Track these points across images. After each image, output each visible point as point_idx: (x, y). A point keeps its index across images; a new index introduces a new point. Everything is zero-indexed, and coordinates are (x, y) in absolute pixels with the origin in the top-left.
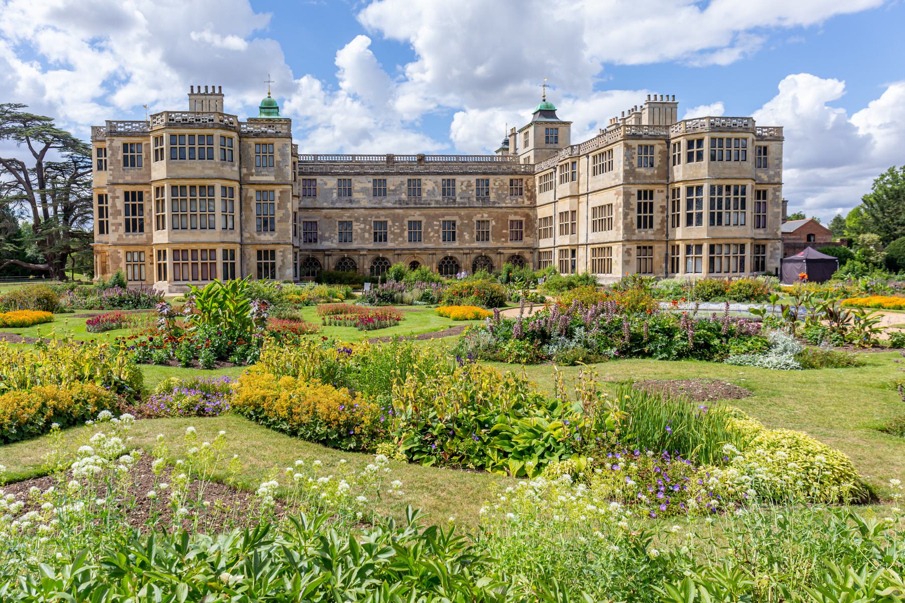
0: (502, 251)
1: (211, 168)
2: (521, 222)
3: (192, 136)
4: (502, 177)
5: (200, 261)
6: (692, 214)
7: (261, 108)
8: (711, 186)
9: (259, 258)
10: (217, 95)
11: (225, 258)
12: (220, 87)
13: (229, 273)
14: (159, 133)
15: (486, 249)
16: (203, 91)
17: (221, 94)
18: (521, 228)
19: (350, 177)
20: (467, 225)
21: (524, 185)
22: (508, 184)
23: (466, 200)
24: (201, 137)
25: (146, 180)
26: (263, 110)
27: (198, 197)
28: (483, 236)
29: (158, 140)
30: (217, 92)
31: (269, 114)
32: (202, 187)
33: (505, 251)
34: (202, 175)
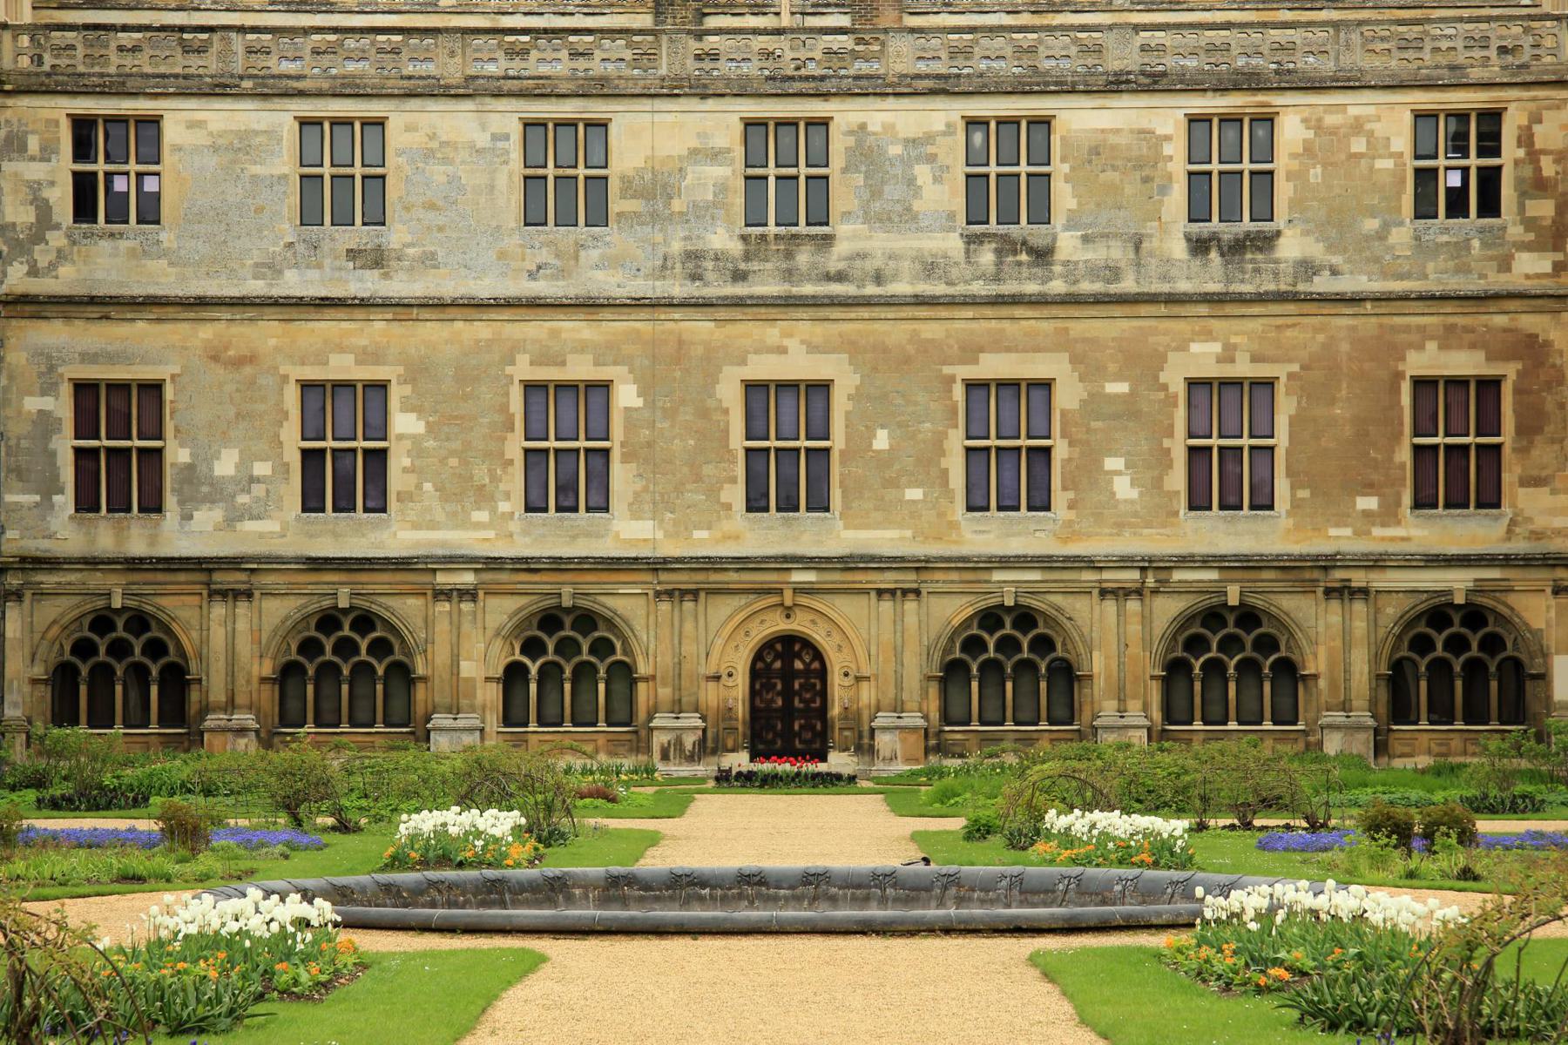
4: (1358, 105)
15: (1248, 564)
19: (373, 109)
22: (1402, 142)
23: (1117, 252)
28: (1222, 479)
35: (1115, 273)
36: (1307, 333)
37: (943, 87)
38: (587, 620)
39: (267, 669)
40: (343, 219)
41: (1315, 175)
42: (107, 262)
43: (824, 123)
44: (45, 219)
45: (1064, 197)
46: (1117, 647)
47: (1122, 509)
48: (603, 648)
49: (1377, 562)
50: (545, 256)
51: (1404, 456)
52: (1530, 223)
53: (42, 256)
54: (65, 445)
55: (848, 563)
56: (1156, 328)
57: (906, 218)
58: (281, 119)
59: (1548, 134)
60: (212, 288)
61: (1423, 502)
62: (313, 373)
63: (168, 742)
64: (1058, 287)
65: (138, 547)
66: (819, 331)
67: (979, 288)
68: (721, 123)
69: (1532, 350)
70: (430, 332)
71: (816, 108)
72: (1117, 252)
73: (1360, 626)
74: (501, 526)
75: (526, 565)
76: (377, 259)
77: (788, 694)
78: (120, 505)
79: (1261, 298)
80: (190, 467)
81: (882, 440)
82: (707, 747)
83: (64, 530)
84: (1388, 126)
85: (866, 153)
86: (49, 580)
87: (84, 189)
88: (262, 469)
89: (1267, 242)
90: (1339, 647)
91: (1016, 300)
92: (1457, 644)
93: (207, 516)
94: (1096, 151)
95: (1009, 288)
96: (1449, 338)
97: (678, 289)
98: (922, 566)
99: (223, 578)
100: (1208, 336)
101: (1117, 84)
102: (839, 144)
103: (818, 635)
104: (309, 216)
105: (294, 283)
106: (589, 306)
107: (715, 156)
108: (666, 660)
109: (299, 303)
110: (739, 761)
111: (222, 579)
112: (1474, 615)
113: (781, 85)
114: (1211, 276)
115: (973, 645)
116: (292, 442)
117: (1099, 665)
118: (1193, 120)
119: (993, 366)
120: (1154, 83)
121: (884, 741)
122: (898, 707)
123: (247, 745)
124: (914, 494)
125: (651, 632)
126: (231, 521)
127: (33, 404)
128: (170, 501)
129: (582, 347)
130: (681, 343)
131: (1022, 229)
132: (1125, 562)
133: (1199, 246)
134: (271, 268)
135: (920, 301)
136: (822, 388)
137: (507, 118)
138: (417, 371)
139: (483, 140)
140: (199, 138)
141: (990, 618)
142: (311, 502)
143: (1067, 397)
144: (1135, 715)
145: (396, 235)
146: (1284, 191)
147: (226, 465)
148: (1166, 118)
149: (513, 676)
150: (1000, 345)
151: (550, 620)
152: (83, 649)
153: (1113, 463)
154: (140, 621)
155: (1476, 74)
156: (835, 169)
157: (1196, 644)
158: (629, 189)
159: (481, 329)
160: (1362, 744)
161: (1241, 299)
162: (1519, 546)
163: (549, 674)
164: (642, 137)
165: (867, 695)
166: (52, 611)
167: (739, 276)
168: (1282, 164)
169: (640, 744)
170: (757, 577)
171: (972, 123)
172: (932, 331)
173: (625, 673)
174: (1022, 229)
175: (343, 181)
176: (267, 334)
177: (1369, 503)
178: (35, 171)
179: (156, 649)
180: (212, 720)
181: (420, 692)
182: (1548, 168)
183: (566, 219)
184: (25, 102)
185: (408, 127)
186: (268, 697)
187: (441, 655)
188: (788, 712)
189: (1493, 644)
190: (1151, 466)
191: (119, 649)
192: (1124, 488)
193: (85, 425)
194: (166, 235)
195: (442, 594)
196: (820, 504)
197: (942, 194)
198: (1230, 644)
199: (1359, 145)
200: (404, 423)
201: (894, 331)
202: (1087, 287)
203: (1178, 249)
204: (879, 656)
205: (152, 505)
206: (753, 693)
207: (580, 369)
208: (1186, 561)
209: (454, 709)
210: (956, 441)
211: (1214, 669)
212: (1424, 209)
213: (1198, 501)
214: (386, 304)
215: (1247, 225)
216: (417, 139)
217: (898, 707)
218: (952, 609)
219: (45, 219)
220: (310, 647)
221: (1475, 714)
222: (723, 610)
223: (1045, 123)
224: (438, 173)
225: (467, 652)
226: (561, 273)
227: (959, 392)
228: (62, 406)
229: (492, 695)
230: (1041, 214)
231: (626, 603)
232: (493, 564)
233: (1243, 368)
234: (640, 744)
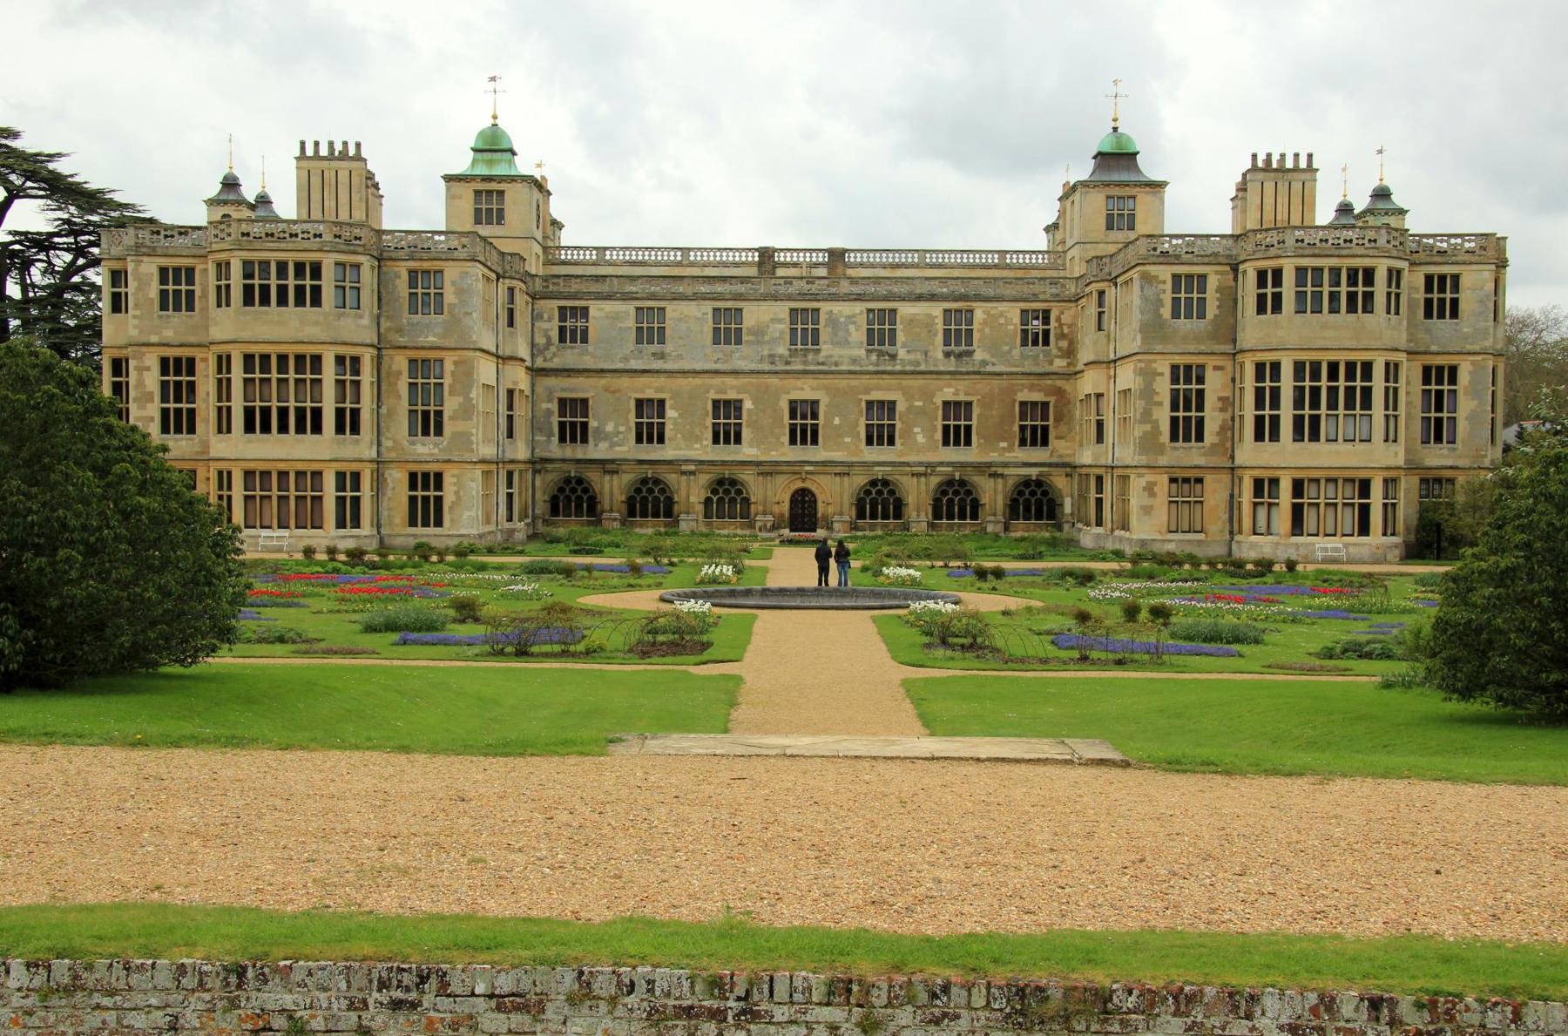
0: (1000, 470)
1: (317, 323)
2: (1045, 405)
3: (282, 267)
4: (1002, 307)
5: (293, 493)
6: (1303, 416)
7: (475, 150)
8: (1296, 363)
9: (413, 486)
10: (352, 159)
11: (341, 486)
12: (358, 145)
13: (349, 514)
14: (223, 256)
16: (324, 152)
17: (358, 157)
18: (1045, 417)
20: (922, 412)
21: (1053, 324)
22: (1017, 320)
24: (300, 268)
25: (204, 340)
26: (479, 155)
27: (292, 375)
28: (957, 435)
29: (223, 268)
30: (352, 152)
31: (490, 163)
32: (300, 358)
33: (1007, 471)
34: (300, 336)
35: (918, 364)
36: (984, 386)
37: (859, 298)
38: (733, 482)
39: (623, 498)
40: (651, 342)
41: (987, 330)
42: (571, 356)
43: (818, 310)
44: (549, 343)
45: (901, 337)
46: (917, 495)
47: (920, 447)
48: (739, 492)
49: (1006, 465)
50: (720, 355)
51: (1016, 428)
52: (1060, 349)
53: (548, 355)
54: (555, 420)
55: (824, 463)
56: (932, 383)
57: (845, 343)
58: (629, 308)
59: (1066, 318)
60: (606, 366)
61: (1023, 443)
62: (640, 396)
63: (590, 523)
64: (898, 368)
65: (580, 456)
66: (816, 382)
67: (871, 368)
68: (782, 309)
69: (1060, 392)
70: (681, 382)
71: (815, 305)
72: (919, 357)
73: (1000, 487)
74: (704, 449)
75: (712, 463)
76: (661, 356)
77: (803, 509)
78: (573, 440)
79: (968, 373)
80: (597, 430)
81: (837, 421)
82: (775, 527)
83: (555, 449)
84: (1013, 312)
85: (832, 321)
86: (549, 466)
87: (562, 330)
88: (622, 429)
89: (970, 354)
90: (993, 495)
91: (884, 372)
92: (1033, 493)
93: (603, 445)
94: (912, 321)
95: (881, 368)
96: (1032, 388)
97: (767, 367)
98: (850, 465)
99: (609, 467)
100: (949, 386)
101: (920, 298)
102: (823, 317)
103: (814, 489)
104: (639, 341)
105: (634, 364)
106: (735, 373)
107: (780, 321)
108: (761, 497)
109: (635, 371)
110: (786, 532)
111: (609, 467)
112: (1039, 483)
113: (803, 296)
114: (951, 365)
115: (868, 492)
116: (632, 419)
117: (911, 500)
118: (945, 311)
119: (876, 396)
120: (932, 297)
121: (836, 525)
122: (841, 514)
123: (616, 525)
124: (848, 440)
125: (757, 488)
126: (612, 445)
127: (545, 406)
128: (591, 439)
129: (733, 387)
130: (767, 387)
131: (886, 347)
132: (920, 464)
133: (947, 355)
134: (626, 359)
135: (850, 372)
136: (815, 403)
137: (708, 307)
138: (676, 395)
139: (699, 315)
140: (602, 314)
141: (873, 483)
142: (639, 440)
143: (900, 407)
144: (923, 517)
145: (669, 347)
146: (976, 336)
147: (610, 428)
148: (936, 310)
149: (708, 501)
150: (879, 388)
151: (720, 482)
152: (561, 490)
153: (917, 430)
154: (580, 481)
155: (1042, 297)
156: (821, 326)
157: (944, 493)
158: (750, 333)
159: (698, 381)
160: (999, 528)
161: (961, 373)
162: (1054, 460)
163: (721, 500)
164: (754, 314)
165: (831, 510)
166: (550, 477)
167: (788, 363)
168: (975, 327)
169: (751, 526)
170: (794, 467)
171: (869, 311)
172: (855, 383)
173: (746, 501)
174: (886, 347)
175: (650, 329)
176: (624, 382)
177: (1003, 444)
178: (546, 325)
179: (586, 490)
180: (605, 515)
181: (676, 507)
182: (1066, 330)
183: (727, 342)
184: (542, 302)
185: (673, 310)
186: (624, 508)
187: (683, 493)
188: (803, 515)
189: (1045, 493)
190: (929, 433)
191: (573, 490)
192: (920, 439)
193: (562, 413)
194: (591, 348)
195: (684, 473)
196: (815, 441)
197: (858, 335)
198: (956, 493)
199: (1002, 321)
200: (671, 413)
201: (842, 383)
202: (908, 368)
203: (940, 355)
204: (835, 497)
205: (585, 440)
206: (791, 508)
207: (732, 395)
208: (941, 464)
209: (688, 513)
210: (863, 422)
211: (951, 501)
212: (1024, 343)
213: (946, 442)
214: (665, 372)
215: (964, 347)
216: (676, 315)
217: (841, 514)
218: (860, 480)
219: (549, 343)
220: (638, 491)
221: (1039, 516)
222: (780, 479)
223: (893, 311)
224: (683, 326)
225: (692, 493)
226: (726, 362)
227: (864, 405)
228: (555, 407)
229: (700, 508)
230: (893, 342)
231: (747, 476)
232: (701, 462)
233: (962, 398)
234: (751, 526)
